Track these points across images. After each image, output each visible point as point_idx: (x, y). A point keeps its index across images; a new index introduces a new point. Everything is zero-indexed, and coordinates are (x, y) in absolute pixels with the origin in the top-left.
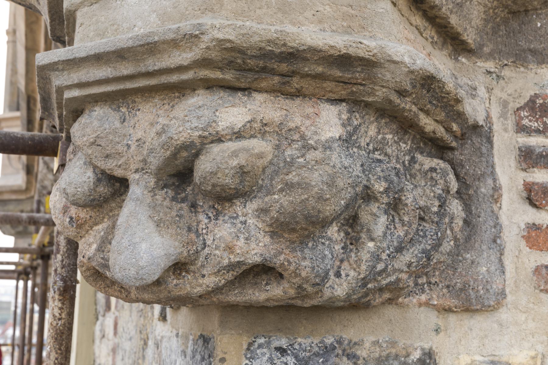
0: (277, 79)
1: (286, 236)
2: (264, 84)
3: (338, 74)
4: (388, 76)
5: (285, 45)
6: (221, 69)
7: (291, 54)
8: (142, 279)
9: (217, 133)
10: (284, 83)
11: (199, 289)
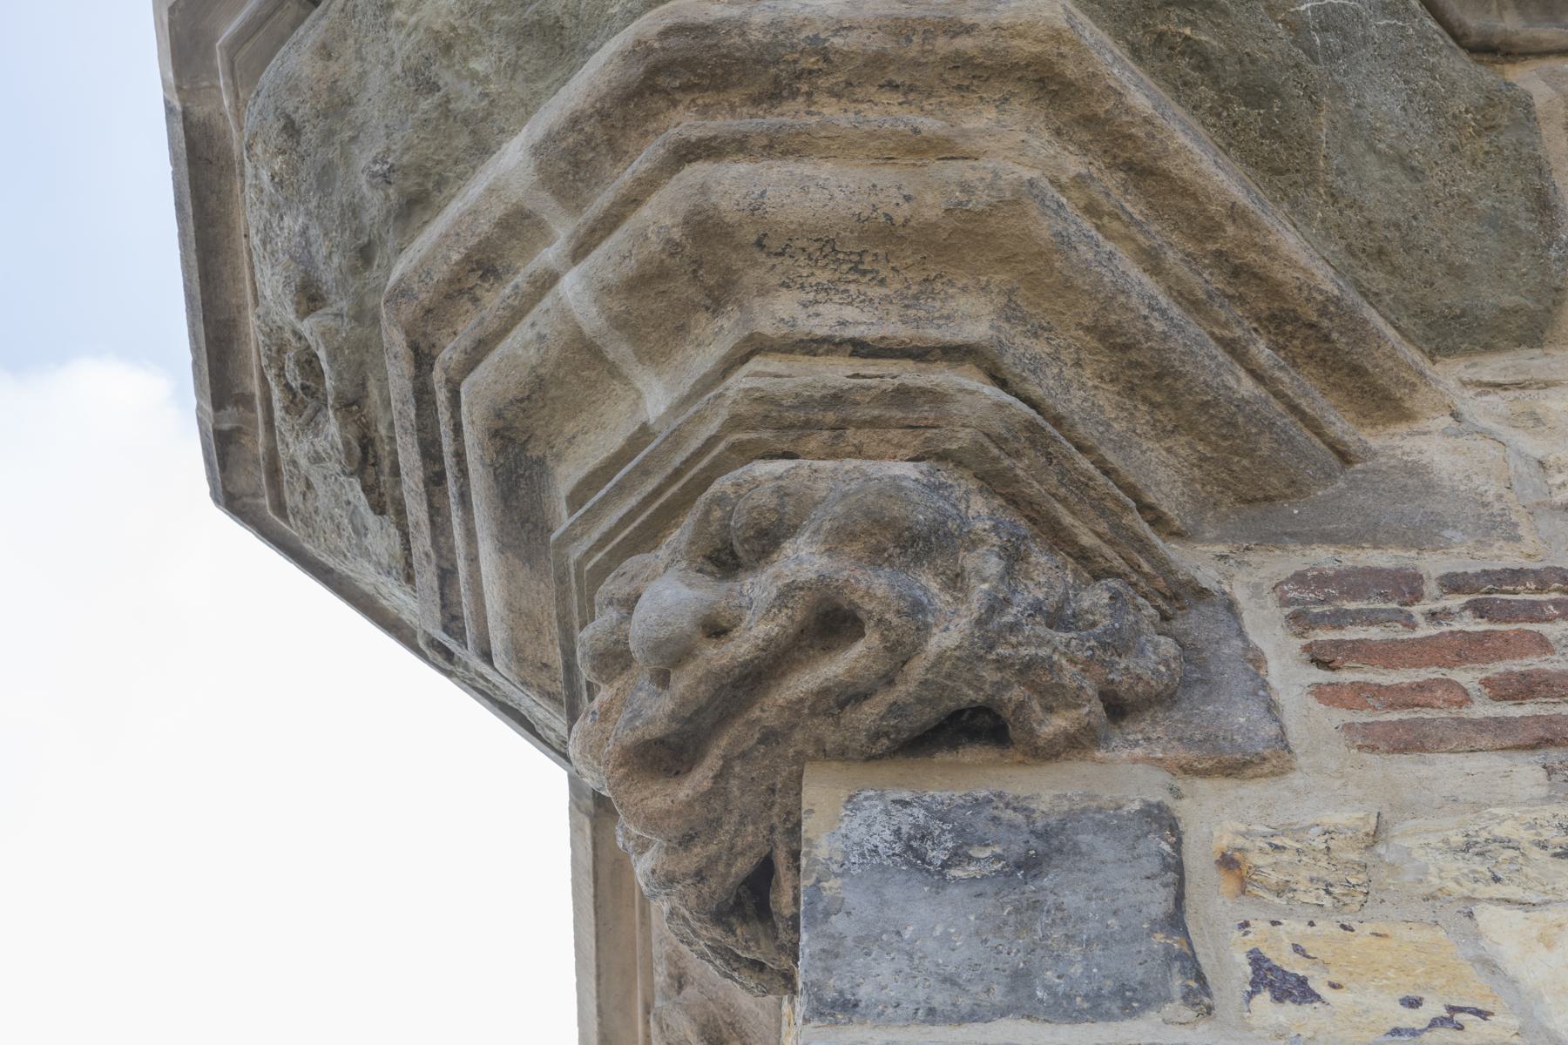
0: (826, 434)
1: (847, 550)
2: (813, 444)
3: (900, 415)
4: (966, 411)
5: (824, 387)
6: (754, 428)
7: (835, 396)
8: (667, 624)
9: (754, 478)
10: (836, 437)
11: (746, 646)
